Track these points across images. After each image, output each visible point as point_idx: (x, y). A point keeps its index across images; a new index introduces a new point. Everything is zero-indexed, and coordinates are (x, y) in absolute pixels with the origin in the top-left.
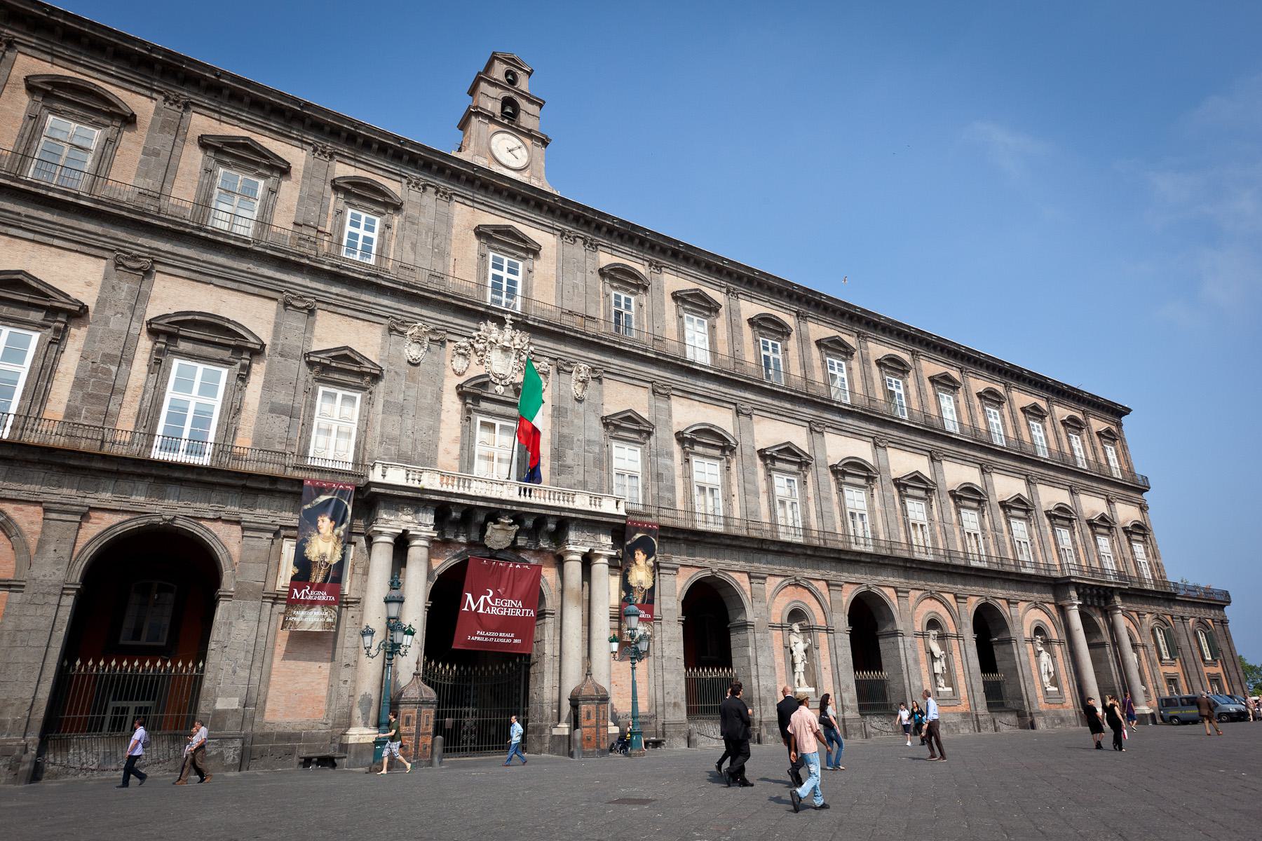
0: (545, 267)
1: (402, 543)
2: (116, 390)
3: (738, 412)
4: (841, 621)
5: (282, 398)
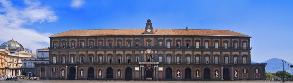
0: (153, 42)
1: (142, 67)
2: (125, 59)
4: (184, 71)
5: (134, 58)
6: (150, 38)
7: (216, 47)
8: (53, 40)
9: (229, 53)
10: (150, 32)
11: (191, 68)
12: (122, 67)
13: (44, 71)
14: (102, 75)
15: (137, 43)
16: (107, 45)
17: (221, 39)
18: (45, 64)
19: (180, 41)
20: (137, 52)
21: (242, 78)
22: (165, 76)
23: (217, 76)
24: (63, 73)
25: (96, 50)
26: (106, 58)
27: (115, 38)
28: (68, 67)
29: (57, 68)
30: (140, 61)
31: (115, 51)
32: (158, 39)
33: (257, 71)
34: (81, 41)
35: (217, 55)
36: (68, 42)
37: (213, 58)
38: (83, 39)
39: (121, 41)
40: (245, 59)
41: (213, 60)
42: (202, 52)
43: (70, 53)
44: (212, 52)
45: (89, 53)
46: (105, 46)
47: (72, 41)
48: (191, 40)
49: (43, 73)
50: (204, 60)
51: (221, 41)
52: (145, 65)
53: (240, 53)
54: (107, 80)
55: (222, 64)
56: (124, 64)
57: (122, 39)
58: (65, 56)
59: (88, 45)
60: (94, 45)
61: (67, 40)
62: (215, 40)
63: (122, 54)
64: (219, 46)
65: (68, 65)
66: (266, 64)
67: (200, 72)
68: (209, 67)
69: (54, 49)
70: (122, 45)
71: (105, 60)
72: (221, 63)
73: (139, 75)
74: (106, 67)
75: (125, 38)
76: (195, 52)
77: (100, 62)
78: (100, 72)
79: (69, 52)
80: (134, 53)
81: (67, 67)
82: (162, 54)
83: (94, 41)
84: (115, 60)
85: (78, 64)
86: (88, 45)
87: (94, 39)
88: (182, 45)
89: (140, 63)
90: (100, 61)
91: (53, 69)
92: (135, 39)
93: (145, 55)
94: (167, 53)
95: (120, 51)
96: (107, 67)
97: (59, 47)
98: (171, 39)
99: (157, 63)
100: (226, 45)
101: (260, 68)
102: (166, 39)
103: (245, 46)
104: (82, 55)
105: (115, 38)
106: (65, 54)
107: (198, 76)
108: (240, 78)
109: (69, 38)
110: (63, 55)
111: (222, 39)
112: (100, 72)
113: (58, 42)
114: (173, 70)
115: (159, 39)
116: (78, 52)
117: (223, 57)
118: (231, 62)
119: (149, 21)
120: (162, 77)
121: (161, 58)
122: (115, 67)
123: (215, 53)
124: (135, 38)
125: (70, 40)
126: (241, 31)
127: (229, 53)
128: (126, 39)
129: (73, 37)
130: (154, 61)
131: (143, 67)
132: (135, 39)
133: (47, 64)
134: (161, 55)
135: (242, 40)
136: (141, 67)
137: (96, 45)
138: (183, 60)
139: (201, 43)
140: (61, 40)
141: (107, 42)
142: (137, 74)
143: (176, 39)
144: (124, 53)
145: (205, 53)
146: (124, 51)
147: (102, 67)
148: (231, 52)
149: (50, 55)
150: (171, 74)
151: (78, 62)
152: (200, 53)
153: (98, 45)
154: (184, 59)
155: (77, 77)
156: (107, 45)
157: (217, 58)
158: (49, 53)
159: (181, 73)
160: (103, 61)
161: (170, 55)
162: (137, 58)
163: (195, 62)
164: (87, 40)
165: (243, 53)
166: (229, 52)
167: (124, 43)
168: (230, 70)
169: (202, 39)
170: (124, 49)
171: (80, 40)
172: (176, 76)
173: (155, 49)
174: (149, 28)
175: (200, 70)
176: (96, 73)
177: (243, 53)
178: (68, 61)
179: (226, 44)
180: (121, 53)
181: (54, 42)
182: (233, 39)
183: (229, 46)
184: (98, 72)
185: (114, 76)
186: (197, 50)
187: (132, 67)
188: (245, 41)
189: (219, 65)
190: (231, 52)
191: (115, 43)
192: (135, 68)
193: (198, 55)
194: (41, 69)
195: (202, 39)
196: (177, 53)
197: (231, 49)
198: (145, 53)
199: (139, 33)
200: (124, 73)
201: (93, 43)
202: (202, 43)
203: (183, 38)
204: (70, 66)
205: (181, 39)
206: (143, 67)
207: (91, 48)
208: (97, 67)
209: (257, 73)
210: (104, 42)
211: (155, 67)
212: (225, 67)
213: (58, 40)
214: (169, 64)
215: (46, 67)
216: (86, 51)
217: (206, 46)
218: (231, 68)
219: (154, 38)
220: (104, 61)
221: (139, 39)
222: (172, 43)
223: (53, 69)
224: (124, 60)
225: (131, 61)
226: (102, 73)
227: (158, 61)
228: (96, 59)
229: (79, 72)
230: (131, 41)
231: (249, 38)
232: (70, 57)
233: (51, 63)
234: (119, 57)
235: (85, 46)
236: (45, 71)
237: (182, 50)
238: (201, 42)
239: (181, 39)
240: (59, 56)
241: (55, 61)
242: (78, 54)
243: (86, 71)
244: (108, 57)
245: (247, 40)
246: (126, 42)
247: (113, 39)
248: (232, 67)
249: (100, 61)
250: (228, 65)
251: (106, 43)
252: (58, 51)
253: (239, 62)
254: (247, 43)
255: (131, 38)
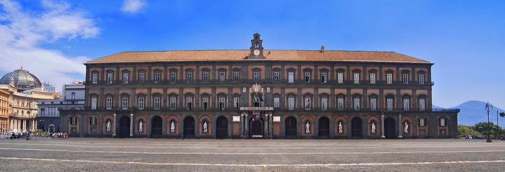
0: (263, 72)
1: (244, 116)
2: (215, 103)
3: (298, 89)
4: (317, 122)
6: (258, 65)
7: (373, 81)
8: (91, 70)
9: (394, 92)
10: (258, 56)
11: (329, 117)
12: (211, 116)
13: (76, 122)
14: (175, 130)
15: (236, 73)
16: (184, 78)
17: (381, 67)
18: (78, 111)
19: (310, 70)
20: (236, 90)
21: (418, 135)
22: (284, 131)
23: (373, 131)
24: (108, 126)
25: (165, 86)
26: (183, 100)
27: (198, 66)
28: (117, 116)
29: (98, 118)
30: (241, 105)
31: (198, 89)
32: (271, 67)
33: (443, 122)
34: (139, 71)
35: (374, 96)
36: (117, 73)
37: (368, 100)
38: (143, 68)
39: (209, 70)
40: (422, 101)
41: (368, 104)
42: (349, 89)
43: (121, 92)
44: (365, 89)
45: (154, 91)
46: (180, 80)
47: (124, 71)
48: (330, 69)
49: (74, 126)
50: (352, 104)
51: (381, 71)
52: (250, 112)
53: (414, 91)
54: (185, 138)
55: (382, 110)
56: (213, 110)
57: (210, 67)
58: (113, 96)
59: (152, 78)
60: (163, 78)
61: (115, 69)
62: (370, 68)
63: (211, 93)
64: (378, 79)
65: (117, 113)
66: (459, 110)
67: (345, 125)
68: (361, 116)
69: (93, 85)
70: (211, 78)
71: (181, 104)
72: (380, 108)
73: (240, 129)
74: (183, 116)
75: (215, 66)
76: (335, 90)
77: (172, 107)
78: (173, 124)
79: (119, 89)
80: (230, 91)
81: (115, 115)
82: (280, 93)
83: (162, 71)
84: (197, 104)
85: (135, 110)
86: (152, 78)
87: (162, 68)
88: (313, 78)
89: (242, 109)
90: (172, 105)
91: (91, 118)
92: (234, 67)
93: (250, 94)
94: (287, 91)
95: (206, 87)
96: (184, 116)
97: (102, 80)
98: (295, 67)
99: (271, 109)
100: (389, 77)
101: (448, 117)
102: (286, 67)
103: (422, 79)
104: (140, 95)
105: (198, 66)
106: (112, 93)
107: (341, 131)
108: (413, 134)
109: (120, 66)
110: (108, 95)
111: (382, 67)
112: (173, 124)
113: (99, 72)
114: (297, 121)
115: (274, 67)
116: (135, 89)
117: (384, 98)
118: (399, 106)
119: (257, 36)
120: (279, 133)
121: (277, 100)
122: (199, 115)
123: (370, 92)
124: (232, 66)
125: (121, 69)
126: (416, 53)
127: (394, 92)
128: (217, 67)
129: (126, 64)
130: (266, 105)
131: (246, 115)
132: (234, 67)
133: (81, 110)
134: (277, 95)
135: (417, 69)
136: (242, 115)
137: (166, 77)
138: (315, 104)
139: (346, 75)
140: (106, 69)
141: (184, 72)
142: (236, 127)
143: (303, 67)
144: (214, 91)
145: (353, 91)
146: (214, 89)
147: (175, 115)
148: (398, 90)
149: (87, 95)
150: (295, 127)
151: (134, 107)
152: (344, 91)
153: (168, 78)
154: (318, 101)
155: (133, 134)
156: (184, 78)
157: (373, 101)
158: (84, 92)
159: (312, 127)
160: (178, 106)
161: (294, 95)
162: (235, 100)
163: (335, 107)
164: (150, 70)
165: (419, 92)
166: (395, 89)
167: (214, 75)
168: (396, 121)
169: (348, 67)
170: (214, 84)
171: (138, 69)
172: (303, 132)
173: (267, 85)
174: (257, 48)
175: (345, 121)
176: (166, 126)
177: (419, 92)
178: (118, 105)
179: (389, 76)
180: (209, 91)
181: (94, 72)
182: (402, 67)
183: (395, 79)
184: (168, 124)
185: (196, 131)
186: (340, 86)
187: (227, 117)
188: (422, 71)
189: (378, 112)
190: (398, 90)
191: (198, 74)
192: (233, 117)
193: (341, 95)
194: (71, 119)
195: (348, 67)
196: (304, 91)
197: (397, 85)
198: (251, 91)
199: (239, 56)
200: (214, 125)
201: (161, 74)
202: (348, 74)
203: (316, 66)
204: (120, 113)
205: (312, 68)
206: (246, 115)
207: (156, 82)
208: (167, 116)
209: (442, 126)
210: (179, 72)
211: (267, 115)
212: (388, 116)
213: (99, 70)
214: (291, 111)
215: (79, 116)
216: (148, 88)
217: (355, 80)
218: (398, 118)
219: (265, 65)
220: (179, 106)
221: (239, 67)
222: (297, 74)
223: (91, 118)
224: (214, 103)
225: (226, 105)
226: (175, 125)
227: (272, 106)
228: (165, 101)
229: (136, 124)
230: (225, 70)
231: (429, 66)
232: (121, 99)
233: (88, 109)
234: (204, 99)
235: (147, 79)
236: (78, 122)
237: (314, 86)
238: (346, 73)
239: (312, 68)
240: (102, 97)
241: (94, 106)
242: (135, 92)
243: (149, 122)
244: (185, 99)
245: (426, 70)
246: (217, 72)
247: (194, 67)
248: (400, 116)
249: (172, 105)
250: (393, 112)
251: (183, 74)
252: (101, 89)
253: (412, 107)
254: (426, 75)
255: (226, 65)
